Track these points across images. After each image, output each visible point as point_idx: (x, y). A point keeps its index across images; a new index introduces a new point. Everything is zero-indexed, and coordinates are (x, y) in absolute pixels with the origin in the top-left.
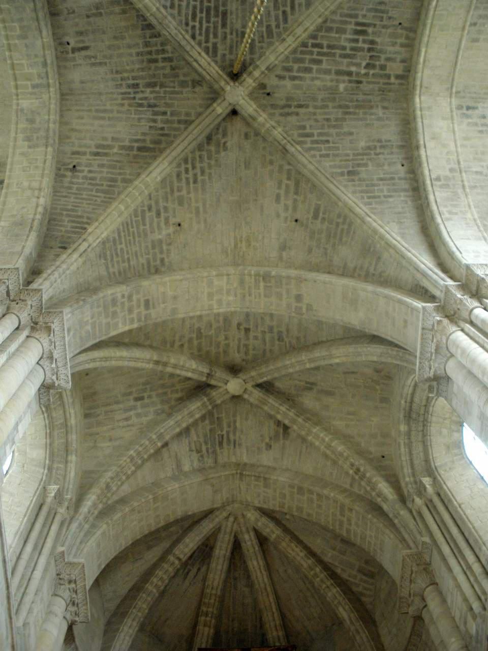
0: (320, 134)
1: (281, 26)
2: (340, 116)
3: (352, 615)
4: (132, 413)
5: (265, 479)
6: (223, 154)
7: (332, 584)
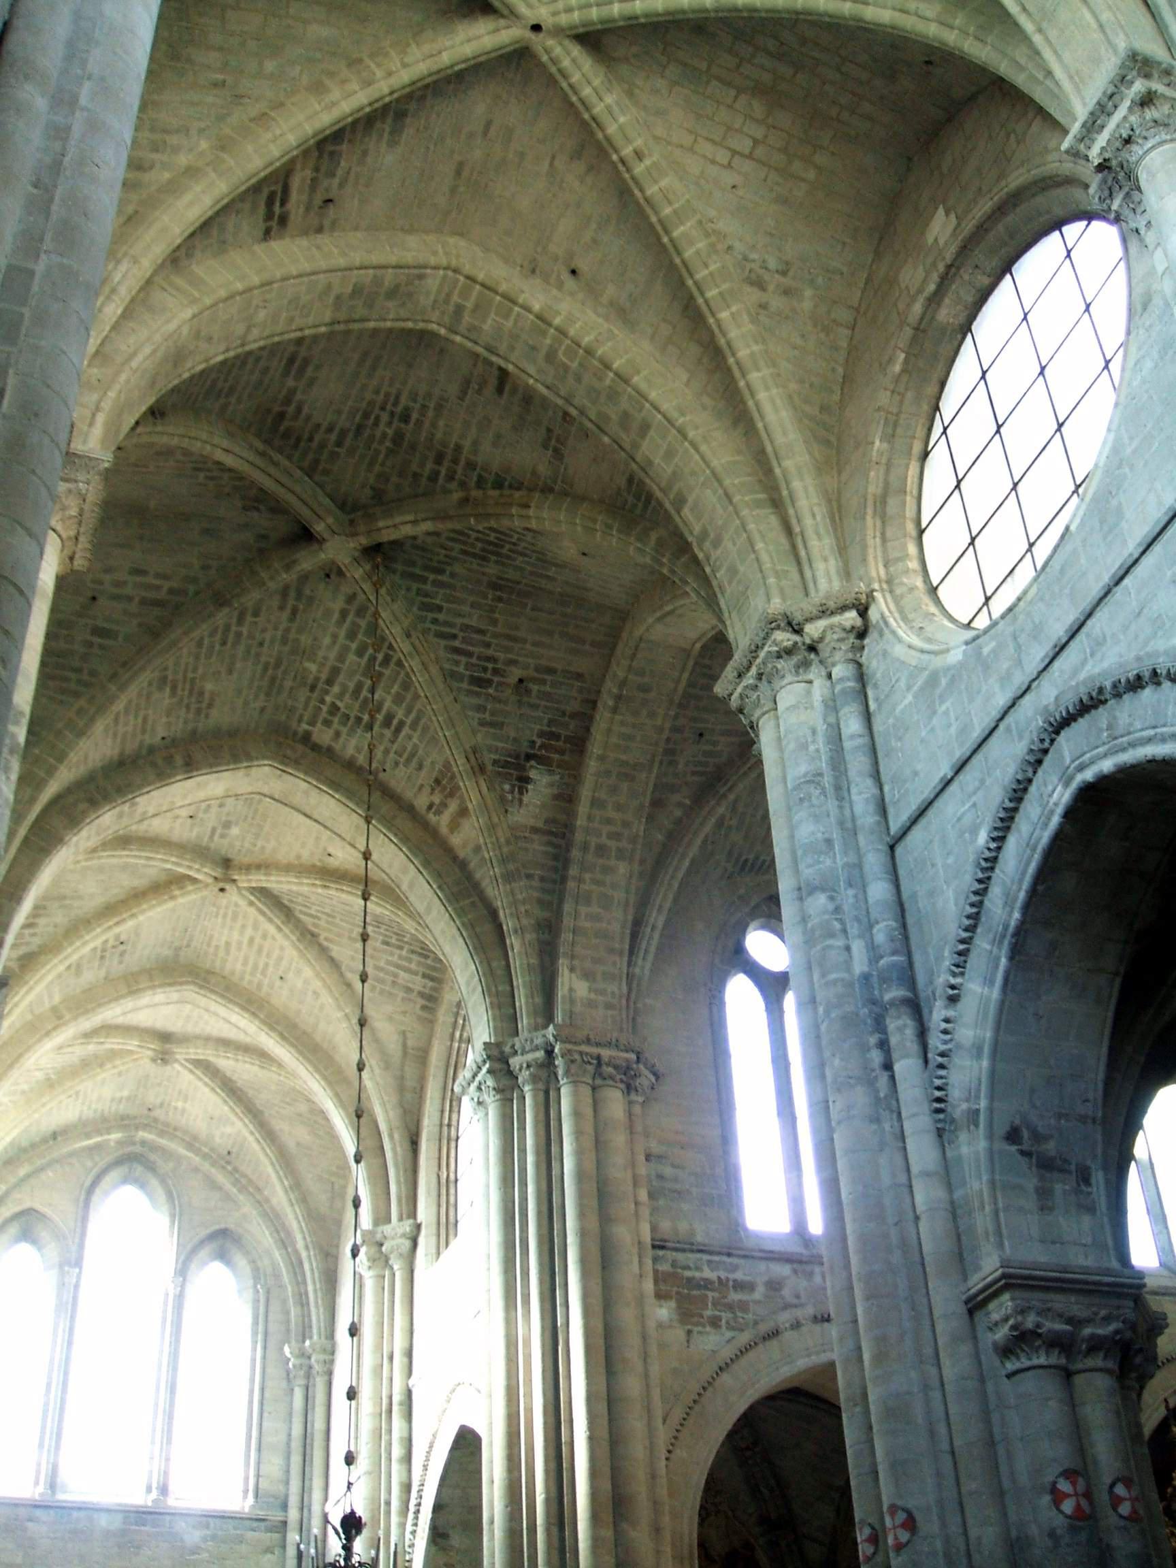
0: (239, 635)
1: (433, 627)
2: (263, 659)
6: (240, 504)
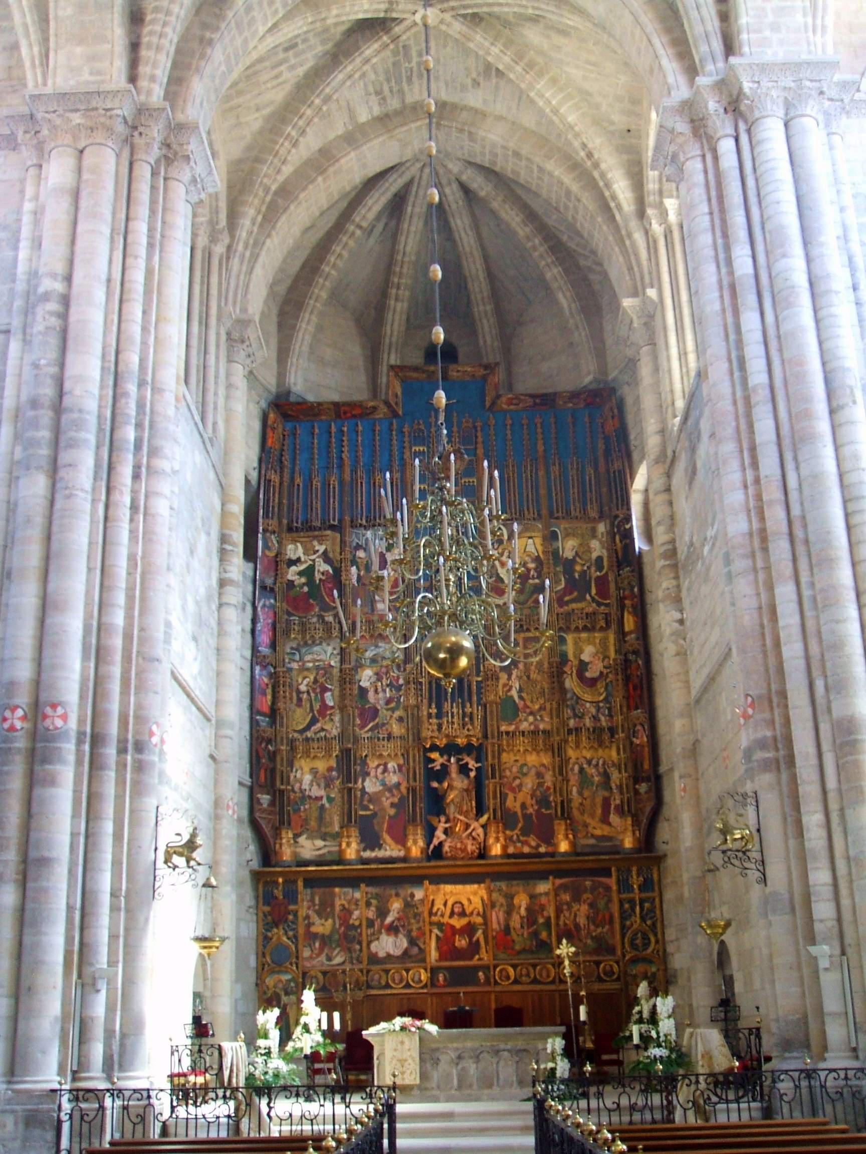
3: (573, 305)
4: (282, 68)
5: (470, 133)
7: (553, 262)
